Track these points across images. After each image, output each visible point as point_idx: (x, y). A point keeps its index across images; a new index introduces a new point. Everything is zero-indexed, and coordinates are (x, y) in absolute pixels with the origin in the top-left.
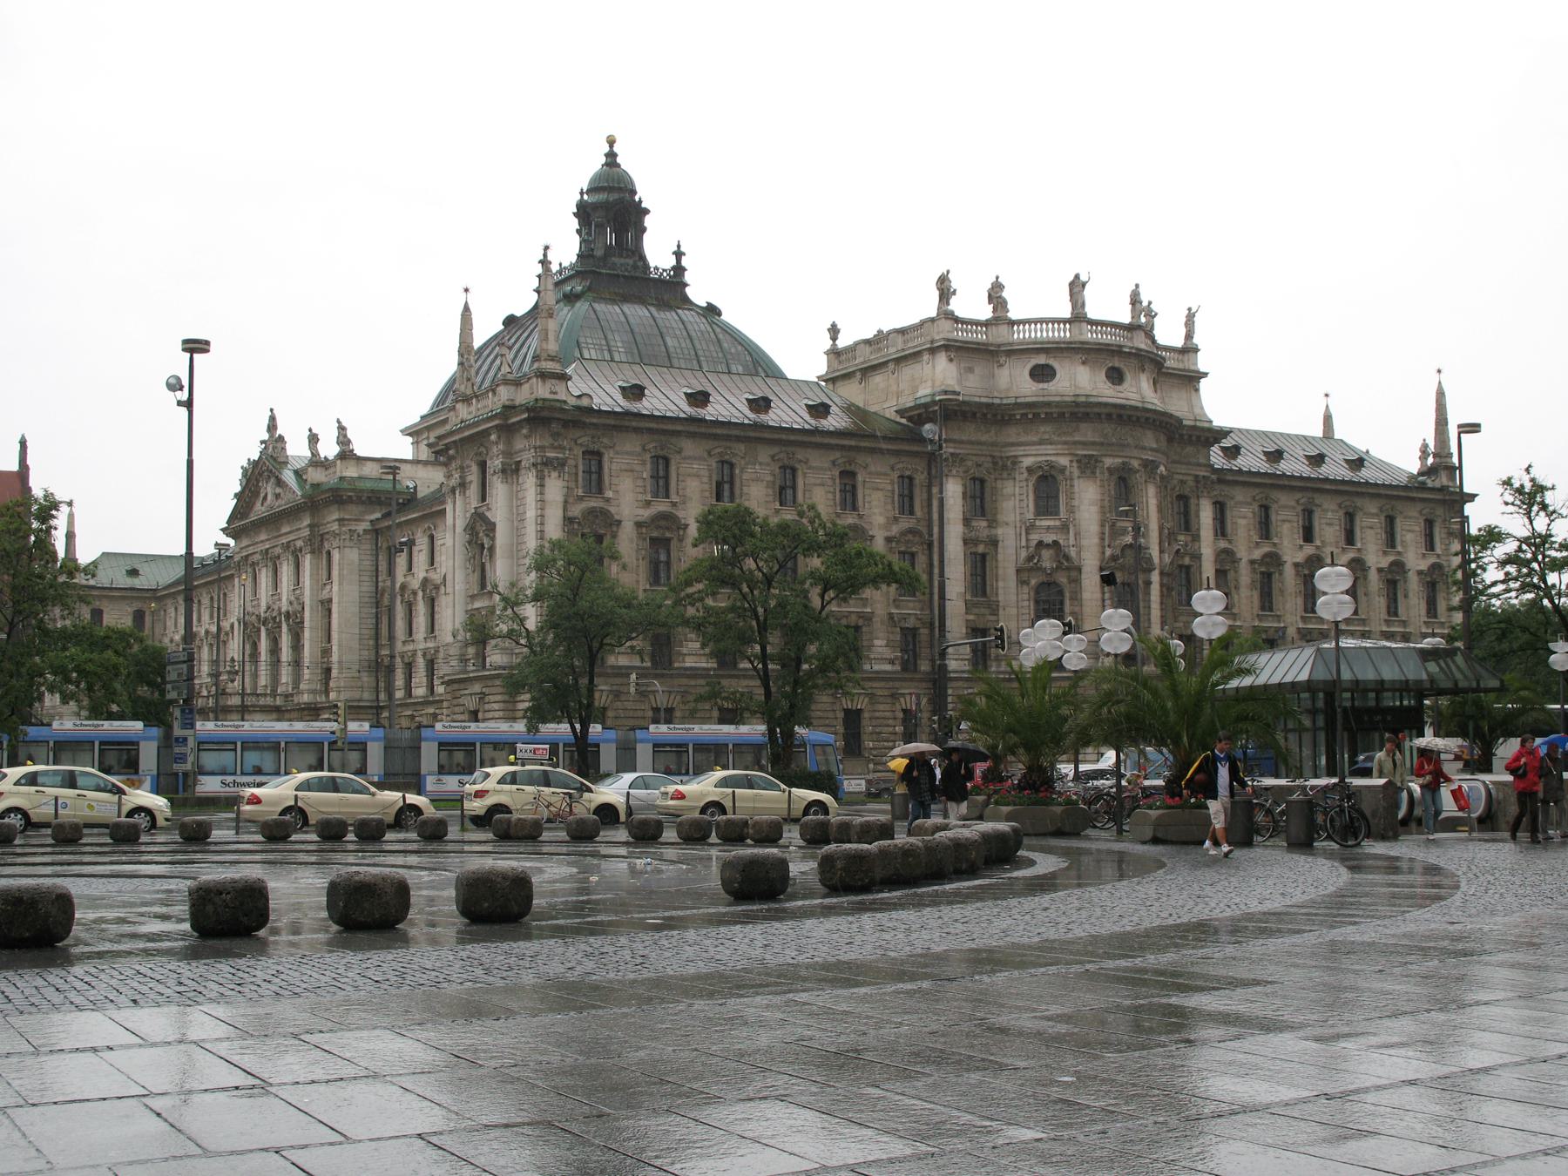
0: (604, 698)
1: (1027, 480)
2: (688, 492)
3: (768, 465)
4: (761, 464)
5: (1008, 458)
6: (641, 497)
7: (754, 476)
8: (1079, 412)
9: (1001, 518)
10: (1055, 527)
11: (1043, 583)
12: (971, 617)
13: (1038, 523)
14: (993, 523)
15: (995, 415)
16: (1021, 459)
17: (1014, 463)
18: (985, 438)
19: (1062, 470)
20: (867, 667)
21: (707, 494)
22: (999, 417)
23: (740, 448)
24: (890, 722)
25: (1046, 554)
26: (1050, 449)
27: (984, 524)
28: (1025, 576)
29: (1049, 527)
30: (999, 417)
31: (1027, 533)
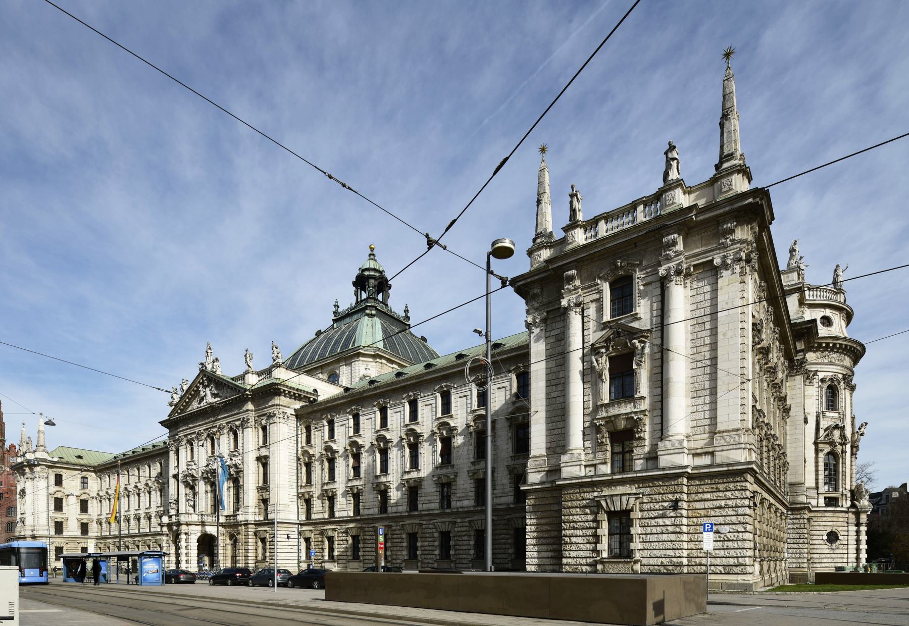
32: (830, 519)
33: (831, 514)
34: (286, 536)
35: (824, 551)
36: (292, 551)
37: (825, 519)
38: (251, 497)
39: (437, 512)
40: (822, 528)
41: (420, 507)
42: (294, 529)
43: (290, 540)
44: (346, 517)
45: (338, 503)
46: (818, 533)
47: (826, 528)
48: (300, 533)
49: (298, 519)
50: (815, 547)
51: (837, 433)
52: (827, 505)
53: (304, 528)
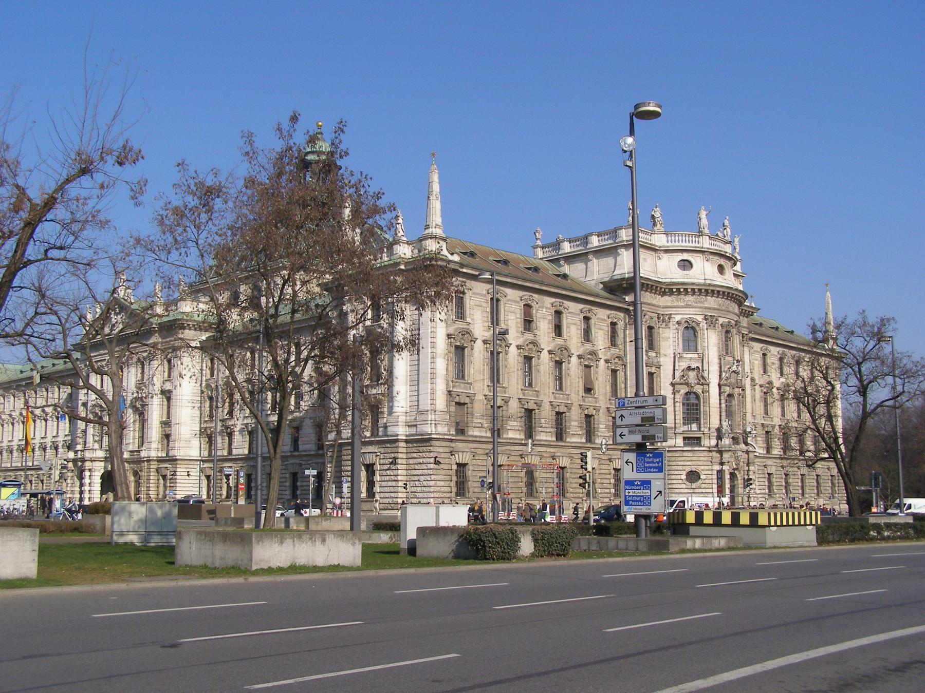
8: (707, 290)
9: (662, 351)
10: (695, 359)
11: (686, 394)
13: (685, 355)
14: (658, 353)
15: (661, 288)
16: (673, 316)
18: (654, 302)
19: (698, 324)
25: (692, 374)
26: (691, 311)
27: (654, 354)
29: (691, 359)
31: (679, 362)
34: (186, 474)
36: (193, 489)
37: (683, 459)
38: (154, 432)
39: (312, 453)
40: (681, 468)
41: (301, 448)
42: (195, 467)
43: (191, 478)
44: (241, 455)
45: (235, 440)
46: (676, 472)
47: (684, 467)
48: (201, 470)
49: (200, 456)
50: (674, 486)
51: (692, 374)
52: (685, 445)
53: (206, 465)
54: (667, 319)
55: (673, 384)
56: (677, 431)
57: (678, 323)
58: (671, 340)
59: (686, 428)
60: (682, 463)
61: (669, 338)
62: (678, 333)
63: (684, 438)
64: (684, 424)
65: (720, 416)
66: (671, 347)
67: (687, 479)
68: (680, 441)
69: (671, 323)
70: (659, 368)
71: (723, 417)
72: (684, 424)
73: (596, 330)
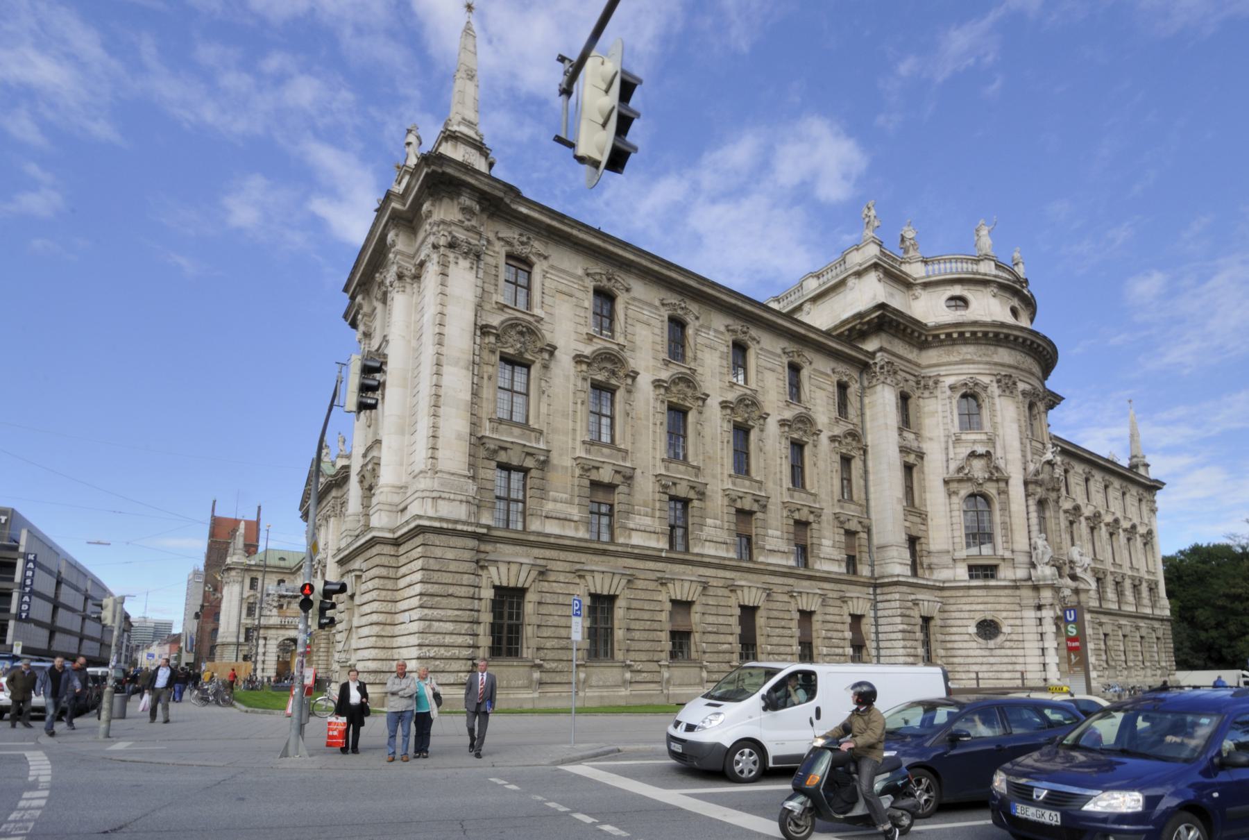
0: (523, 575)
1: (950, 398)
2: (638, 339)
3: (722, 333)
4: (716, 331)
5: (930, 377)
6: (585, 330)
7: (708, 342)
12: (907, 524)
17: (936, 383)
20: (818, 566)
21: (659, 348)
22: (923, 338)
23: (694, 307)
24: (839, 627)
28: (954, 486)
30: (923, 338)
31: (954, 447)
32: (980, 600)
33: (981, 592)
35: (971, 653)
37: (971, 600)
40: (966, 615)
50: (956, 645)
54: (931, 383)
55: (946, 482)
56: (958, 555)
57: (952, 388)
58: (940, 414)
59: (974, 551)
60: (967, 607)
61: (937, 412)
62: (951, 403)
63: (971, 568)
64: (968, 545)
65: (1029, 532)
66: (941, 425)
67: (978, 634)
68: (962, 573)
69: (939, 389)
70: (922, 458)
71: (1034, 534)
72: (968, 545)
73: (813, 388)
